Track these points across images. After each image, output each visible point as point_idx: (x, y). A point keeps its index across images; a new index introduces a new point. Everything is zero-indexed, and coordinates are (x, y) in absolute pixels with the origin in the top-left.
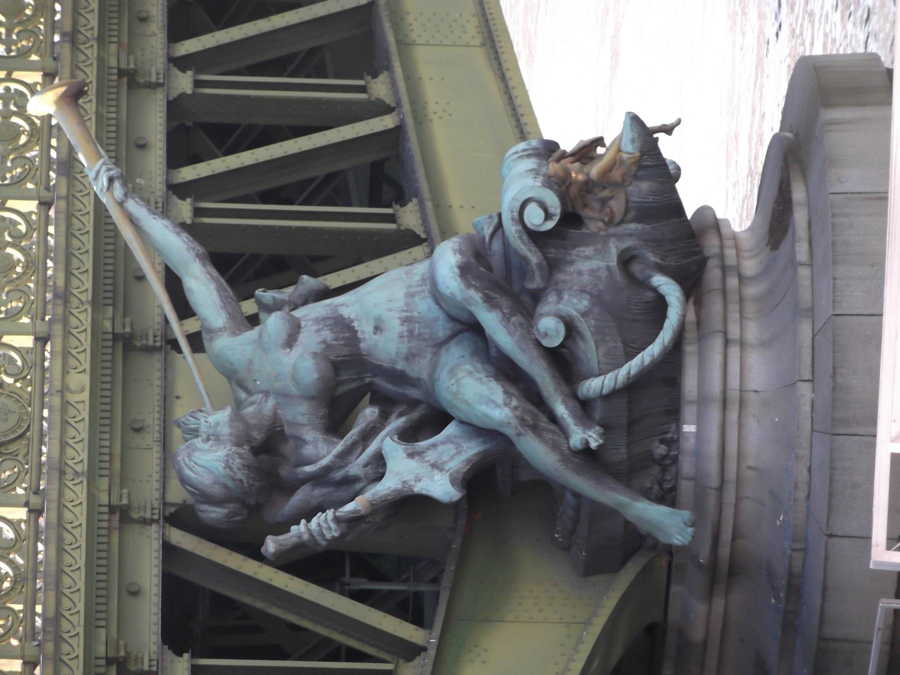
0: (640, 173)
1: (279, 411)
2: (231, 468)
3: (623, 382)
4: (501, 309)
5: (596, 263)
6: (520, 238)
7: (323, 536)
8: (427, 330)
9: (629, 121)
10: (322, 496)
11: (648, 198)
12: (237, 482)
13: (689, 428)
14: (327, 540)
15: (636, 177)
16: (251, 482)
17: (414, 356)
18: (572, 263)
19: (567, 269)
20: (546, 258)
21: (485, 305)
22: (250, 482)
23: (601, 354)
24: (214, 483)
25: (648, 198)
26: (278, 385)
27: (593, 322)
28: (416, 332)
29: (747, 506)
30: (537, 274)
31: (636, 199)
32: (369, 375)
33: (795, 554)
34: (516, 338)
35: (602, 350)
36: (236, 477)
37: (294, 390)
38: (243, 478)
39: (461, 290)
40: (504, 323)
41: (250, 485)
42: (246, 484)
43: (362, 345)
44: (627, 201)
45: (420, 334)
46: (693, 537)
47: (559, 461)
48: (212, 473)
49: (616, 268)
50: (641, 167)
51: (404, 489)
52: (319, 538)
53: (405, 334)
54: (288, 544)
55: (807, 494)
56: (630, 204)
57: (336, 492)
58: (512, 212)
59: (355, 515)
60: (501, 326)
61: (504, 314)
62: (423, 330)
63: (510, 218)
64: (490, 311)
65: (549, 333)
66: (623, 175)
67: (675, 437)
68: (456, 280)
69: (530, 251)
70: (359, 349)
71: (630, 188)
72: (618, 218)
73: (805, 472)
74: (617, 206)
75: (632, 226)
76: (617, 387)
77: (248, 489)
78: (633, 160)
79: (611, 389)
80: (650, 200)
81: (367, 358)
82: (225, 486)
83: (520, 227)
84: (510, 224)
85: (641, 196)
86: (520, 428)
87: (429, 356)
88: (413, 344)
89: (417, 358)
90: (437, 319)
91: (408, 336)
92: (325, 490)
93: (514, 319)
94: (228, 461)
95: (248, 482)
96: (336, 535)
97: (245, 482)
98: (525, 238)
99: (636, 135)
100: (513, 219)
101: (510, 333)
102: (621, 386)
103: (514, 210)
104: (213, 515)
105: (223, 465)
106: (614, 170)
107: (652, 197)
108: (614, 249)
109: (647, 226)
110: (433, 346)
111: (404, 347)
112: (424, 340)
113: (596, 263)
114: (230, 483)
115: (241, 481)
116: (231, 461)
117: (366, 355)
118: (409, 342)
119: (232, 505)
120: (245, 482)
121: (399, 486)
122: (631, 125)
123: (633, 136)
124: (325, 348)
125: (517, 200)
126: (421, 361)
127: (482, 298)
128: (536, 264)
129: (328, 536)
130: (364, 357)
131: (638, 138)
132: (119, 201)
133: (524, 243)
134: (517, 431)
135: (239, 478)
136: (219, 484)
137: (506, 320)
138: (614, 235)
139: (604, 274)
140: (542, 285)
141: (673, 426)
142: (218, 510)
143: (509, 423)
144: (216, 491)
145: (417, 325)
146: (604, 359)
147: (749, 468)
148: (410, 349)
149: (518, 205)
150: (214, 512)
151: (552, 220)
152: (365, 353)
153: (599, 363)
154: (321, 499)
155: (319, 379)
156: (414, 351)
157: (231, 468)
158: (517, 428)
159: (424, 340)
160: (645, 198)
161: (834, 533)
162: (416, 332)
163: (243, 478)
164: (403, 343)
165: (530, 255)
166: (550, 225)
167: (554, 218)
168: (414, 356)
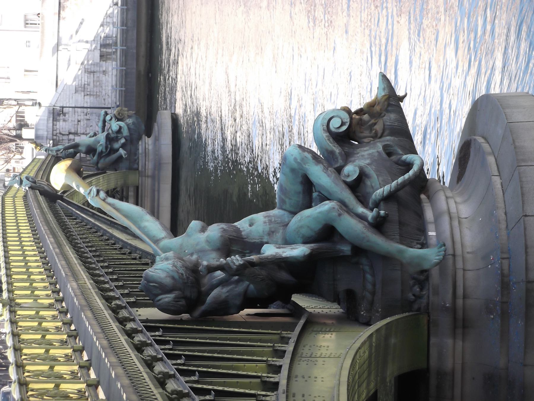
0: (390, 108)
1: (200, 261)
2: (176, 267)
3: (395, 187)
4: (323, 164)
5: (371, 151)
6: (329, 140)
7: (234, 263)
8: (279, 219)
9: (381, 77)
10: (227, 292)
11: (395, 123)
12: (180, 274)
13: (432, 234)
14: (236, 266)
15: (387, 111)
16: (188, 276)
17: (273, 232)
18: (358, 153)
19: (356, 156)
20: (344, 151)
21: (314, 161)
22: (188, 276)
23: (380, 180)
24: (166, 277)
25: (395, 123)
26: (198, 247)
27: (374, 167)
28: (273, 220)
29: (470, 275)
30: (339, 158)
31: (388, 123)
32: (248, 251)
33: (504, 261)
34: (332, 178)
35: (381, 179)
36: (179, 272)
37: (207, 247)
38: (183, 272)
39: (300, 153)
40: (325, 171)
41: (188, 278)
42: (185, 277)
43: (243, 233)
44: (384, 125)
45: (275, 221)
46: (443, 257)
47: (364, 227)
48: (166, 271)
49: (382, 151)
50: (389, 105)
51: (277, 255)
52: (231, 264)
53: (267, 221)
54: (215, 264)
55: (506, 226)
56: (386, 126)
57: (236, 287)
58: (323, 126)
59: (251, 260)
60: (324, 173)
61: (324, 166)
62: (277, 219)
63: (322, 129)
64: (316, 165)
65: (350, 174)
66: (381, 110)
67: (425, 242)
68: (297, 149)
69: (334, 146)
70: (241, 235)
71: (385, 118)
72: (379, 135)
73: (504, 215)
74: (379, 127)
75: (388, 138)
76: (391, 190)
77: (186, 281)
78: (386, 97)
79: (388, 191)
80: (396, 124)
81: (246, 240)
82: (173, 278)
83: (328, 134)
84: (323, 133)
85: (391, 122)
86: (340, 210)
87: (281, 231)
88: (272, 226)
89: (275, 234)
90: (284, 214)
91: (268, 222)
92: (229, 288)
93: (330, 169)
94: (174, 263)
95: (186, 275)
96: (241, 263)
97: (184, 275)
98: (331, 140)
99: (386, 86)
100: (324, 130)
101: (328, 176)
102: (394, 189)
103: (324, 125)
104: (166, 300)
105: (172, 266)
106: (375, 106)
107: (398, 123)
108: (380, 146)
109: (396, 138)
110: (283, 226)
111: (267, 228)
112: (278, 223)
113: (371, 151)
114: (176, 276)
115: (182, 274)
116: (175, 263)
117: (246, 238)
118: (270, 225)
119: (177, 292)
120: (184, 275)
121: (274, 254)
122: (382, 79)
123: (384, 86)
124: (223, 231)
125: (325, 119)
126: (277, 234)
127: (312, 157)
128: (339, 153)
129: (237, 263)
130: (245, 240)
131: (387, 87)
132: (103, 199)
133: (331, 142)
134: (339, 212)
135: (181, 272)
136: (169, 277)
137: (326, 169)
138: (380, 142)
139: (376, 154)
140: (343, 164)
141: (423, 238)
142: (169, 295)
143: (334, 208)
144: (168, 281)
145: (273, 218)
146: (382, 183)
147: (468, 253)
148: (270, 228)
149: (326, 122)
150: (167, 297)
151: (345, 125)
152: (245, 237)
153: (380, 184)
154: (227, 294)
155: (222, 236)
156: (273, 230)
157: (176, 267)
158: (339, 211)
159: (278, 223)
160: (393, 123)
161: (528, 214)
162: (273, 220)
163: (183, 272)
164: (266, 225)
165: (334, 149)
166: (344, 128)
167: (346, 124)
168: (273, 232)
